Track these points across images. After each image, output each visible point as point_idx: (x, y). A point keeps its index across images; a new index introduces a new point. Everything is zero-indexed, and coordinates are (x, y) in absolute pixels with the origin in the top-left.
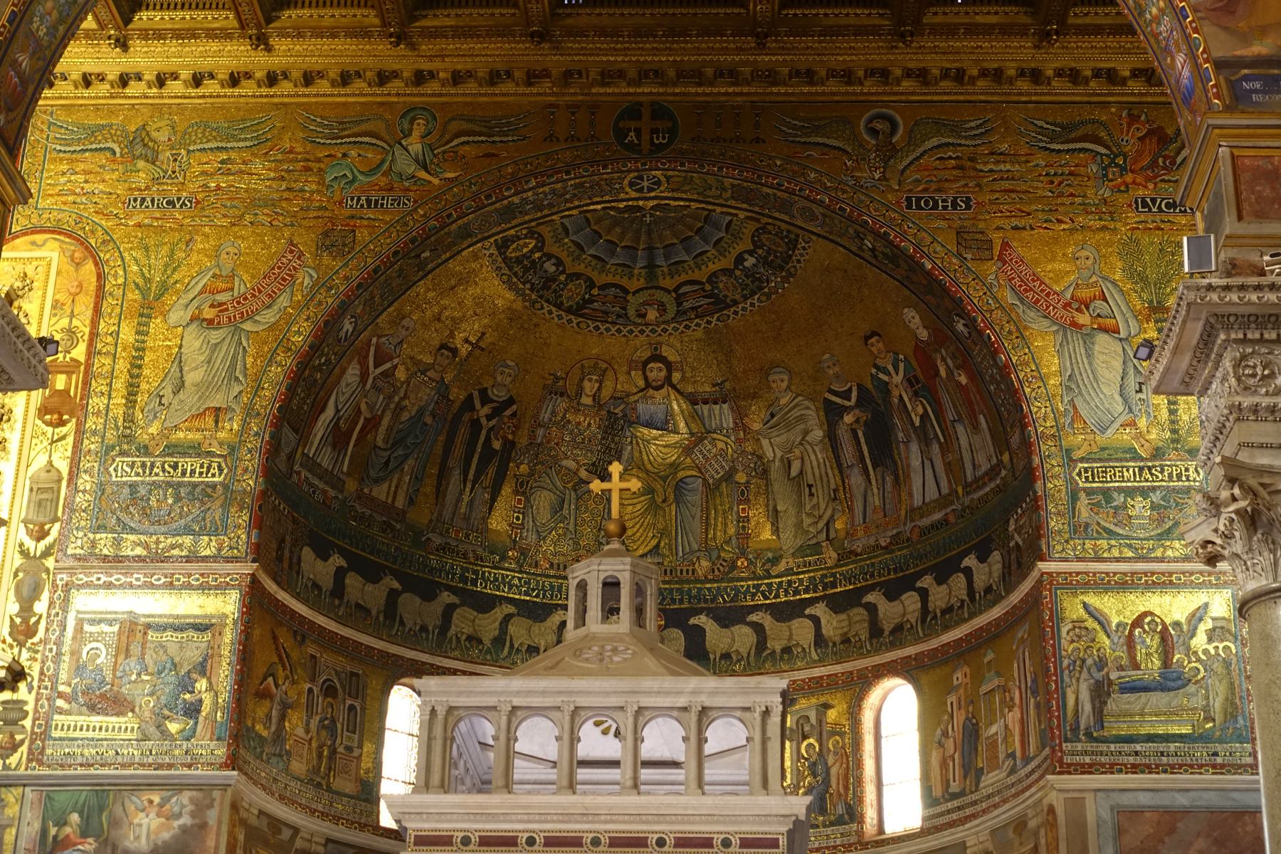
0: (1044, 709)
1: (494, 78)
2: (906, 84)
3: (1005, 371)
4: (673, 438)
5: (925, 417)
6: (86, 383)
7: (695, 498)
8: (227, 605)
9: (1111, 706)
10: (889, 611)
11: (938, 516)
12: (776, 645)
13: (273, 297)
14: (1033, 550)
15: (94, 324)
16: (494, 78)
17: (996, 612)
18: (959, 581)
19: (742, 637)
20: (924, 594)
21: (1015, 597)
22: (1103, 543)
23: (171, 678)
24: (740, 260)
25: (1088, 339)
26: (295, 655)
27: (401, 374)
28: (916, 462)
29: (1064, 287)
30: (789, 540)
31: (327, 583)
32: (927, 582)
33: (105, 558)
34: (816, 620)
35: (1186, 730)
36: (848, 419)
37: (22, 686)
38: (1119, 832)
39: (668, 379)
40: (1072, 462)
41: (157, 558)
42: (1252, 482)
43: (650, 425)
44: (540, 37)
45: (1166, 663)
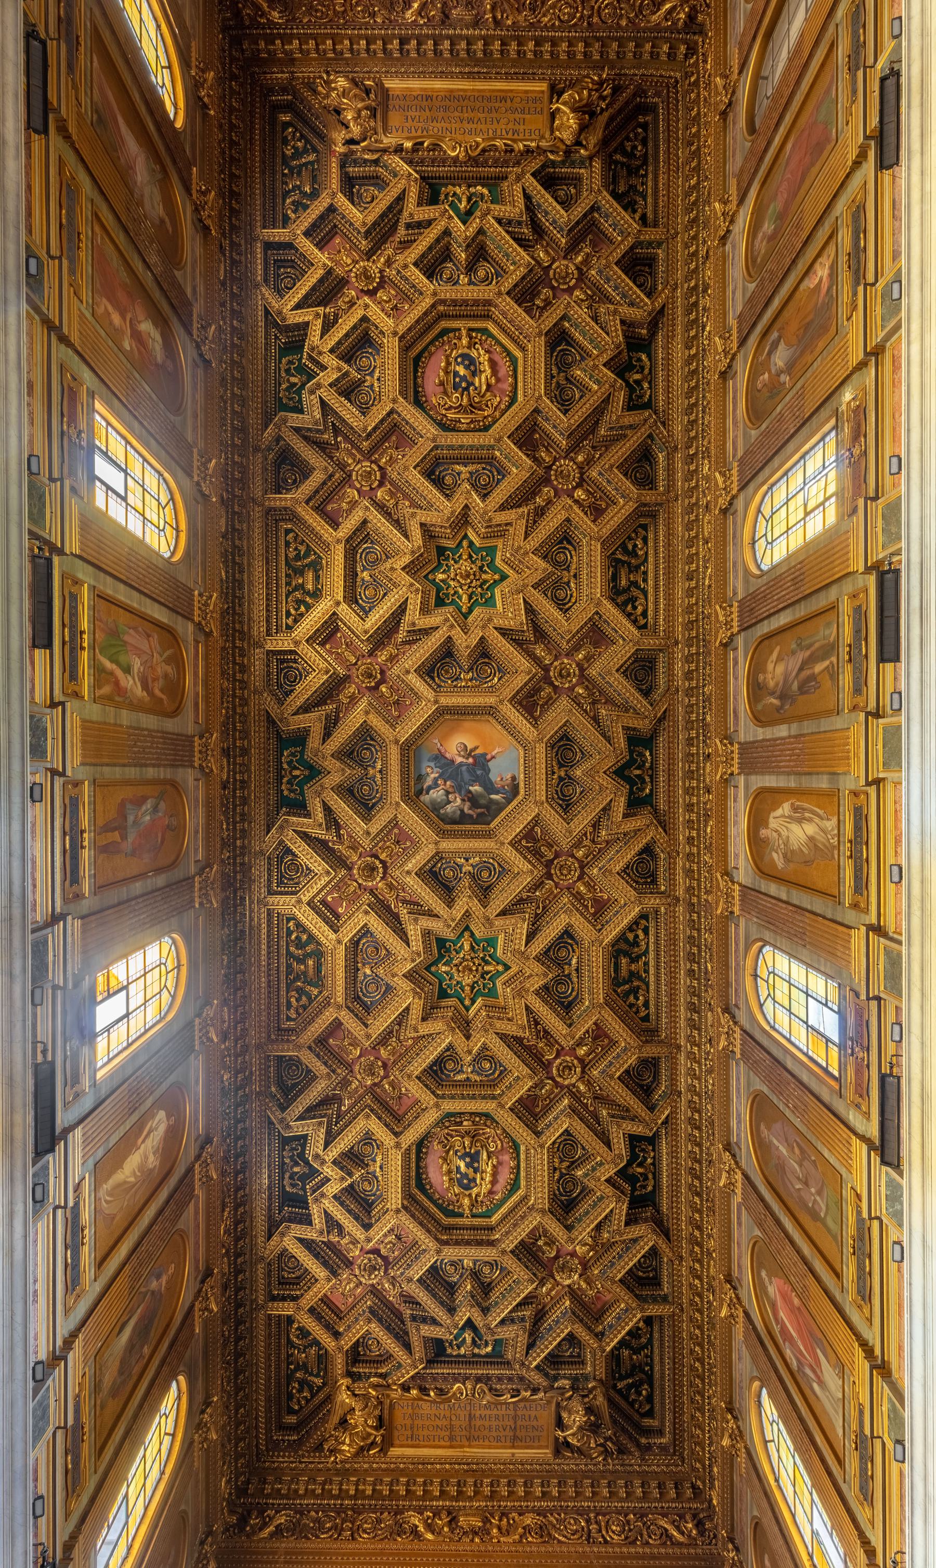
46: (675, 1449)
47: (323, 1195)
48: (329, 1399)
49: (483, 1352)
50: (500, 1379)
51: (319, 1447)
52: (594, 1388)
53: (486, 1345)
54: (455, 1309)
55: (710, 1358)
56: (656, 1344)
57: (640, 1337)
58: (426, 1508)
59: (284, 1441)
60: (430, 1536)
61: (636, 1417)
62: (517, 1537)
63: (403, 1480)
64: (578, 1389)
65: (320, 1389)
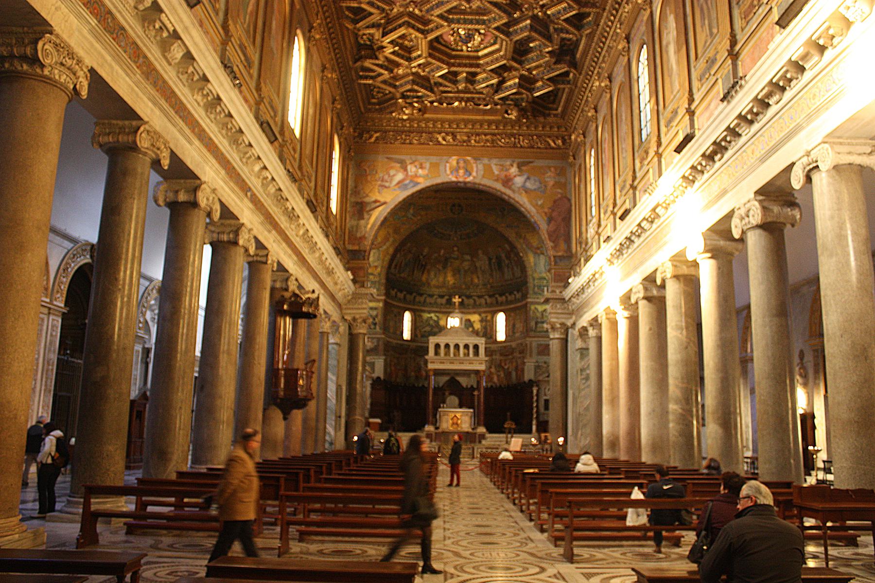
3: (523, 261)
7: (462, 272)
8: (381, 305)
10: (500, 299)
11: (509, 282)
12: (477, 303)
13: (385, 244)
14: (525, 296)
18: (513, 296)
19: (471, 301)
20: (507, 297)
21: (524, 302)
32: (507, 294)
36: (494, 261)
38: (538, 348)
39: (458, 250)
40: (534, 279)
43: (454, 258)
46: (563, 114)
47: (384, 52)
50: (479, 99)
60: (444, 143)
65: (387, 94)
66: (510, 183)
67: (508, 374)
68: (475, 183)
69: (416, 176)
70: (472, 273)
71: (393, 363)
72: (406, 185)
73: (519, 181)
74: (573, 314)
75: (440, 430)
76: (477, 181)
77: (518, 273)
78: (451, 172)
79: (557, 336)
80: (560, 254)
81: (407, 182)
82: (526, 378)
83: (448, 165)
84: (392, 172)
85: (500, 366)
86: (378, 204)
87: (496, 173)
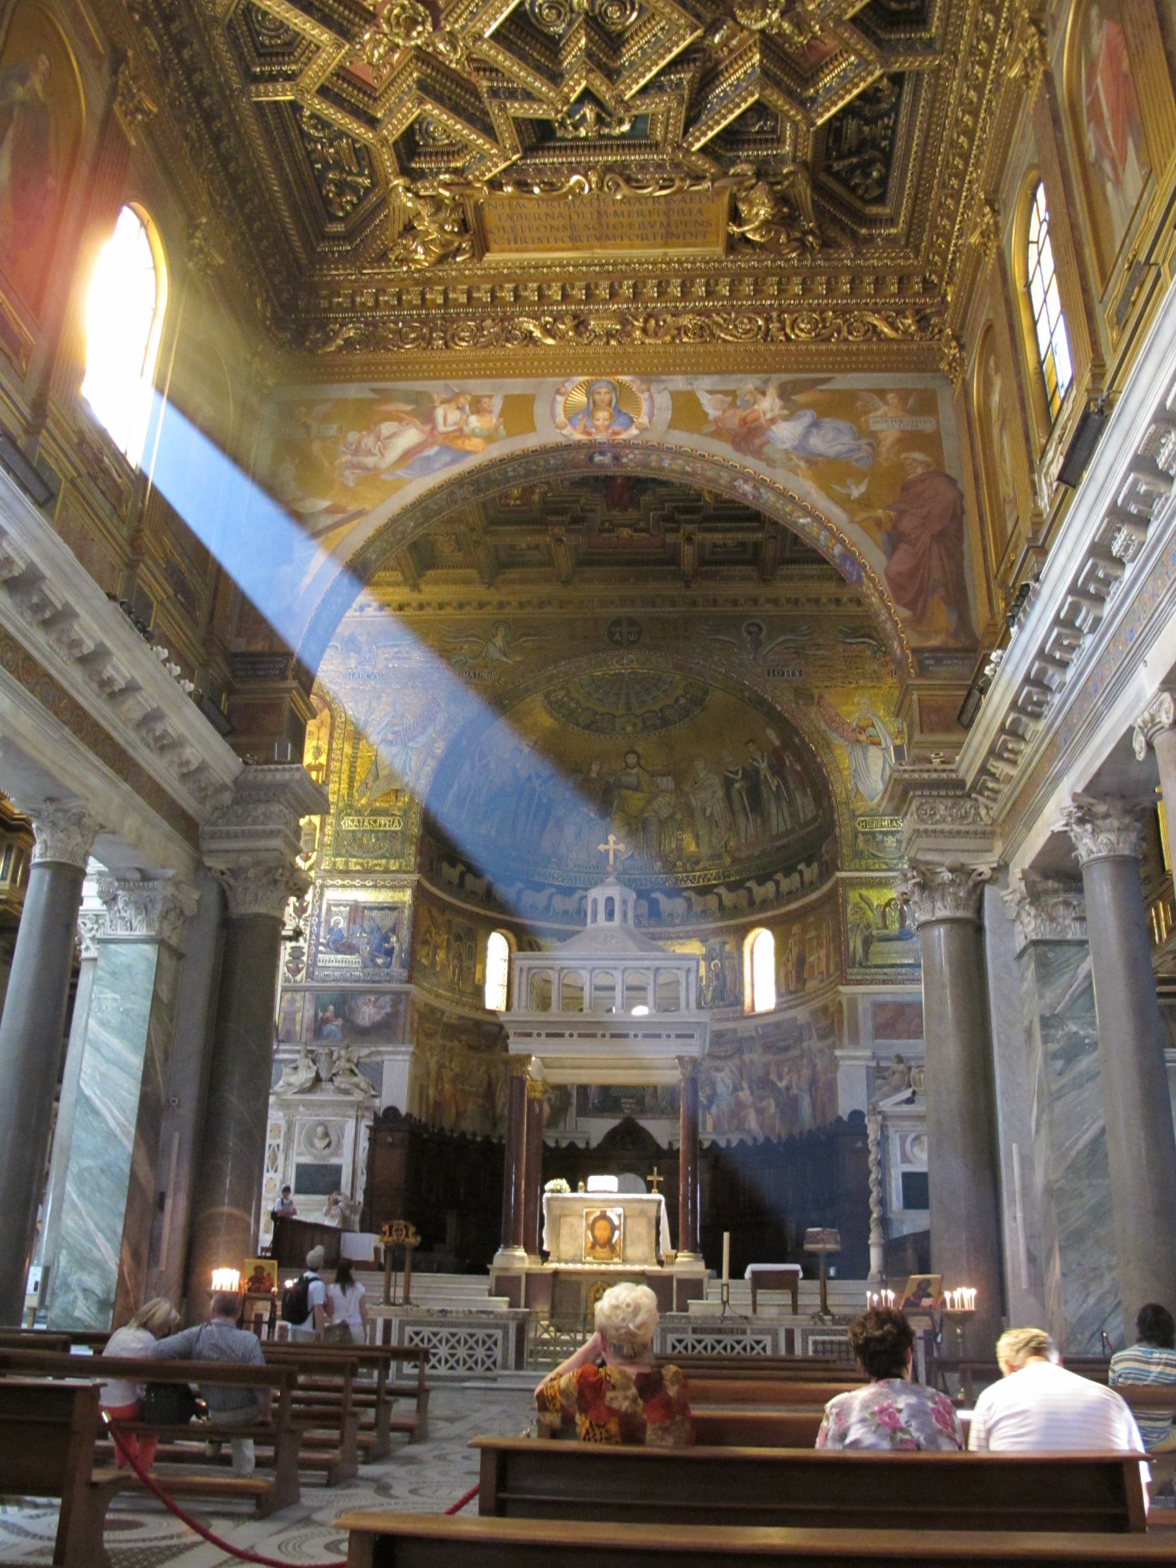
0: (838, 950)
1: (542, 605)
2: (768, 607)
3: (820, 767)
4: (639, 795)
5: (778, 787)
6: (327, 776)
8: (407, 896)
9: (873, 948)
11: (785, 841)
13: (424, 728)
15: (330, 744)
16: (542, 605)
17: (814, 896)
18: (796, 877)
20: (777, 883)
22: (870, 862)
23: (377, 935)
24: (677, 700)
25: (865, 750)
26: (440, 920)
27: (492, 765)
28: (774, 811)
29: (853, 720)
30: (705, 851)
31: (456, 880)
33: (340, 872)
34: (719, 896)
35: (911, 961)
36: (737, 785)
37: (301, 939)
38: (875, 1015)
39: (638, 764)
40: (854, 816)
41: (367, 872)
42: (923, 868)
43: (628, 788)
44: (566, 583)
45: (902, 924)
48: (383, 202)
49: (617, 131)
50: (643, 166)
51: (383, 257)
52: (790, 173)
53: (621, 122)
54: (562, 76)
55: (983, 131)
56: (904, 111)
57: (879, 101)
58: (543, 313)
59: (333, 253)
61: (858, 204)
62: (668, 338)
63: (510, 286)
64: (767, 175)
65: (368, 190)
66: (757, 442)
67: (789, 1106)
68: (647, 448)
69: (460, 433)
70: (680, 828)
71: (447, 1074)
72: (428, 459)
73: (785, 433)
74: (993, 833)
75: (551, 1266)
76: (653, 438)
77: (805, 805)
78: (570, 420)
79: (943, 912)
80: (934, 642)
81: (432, 451)
82: (844, 1108)
83: (559, 398)
84: (386, 428)
85: (763, 1084)
86: (339, 516)
87: (713, 413)
